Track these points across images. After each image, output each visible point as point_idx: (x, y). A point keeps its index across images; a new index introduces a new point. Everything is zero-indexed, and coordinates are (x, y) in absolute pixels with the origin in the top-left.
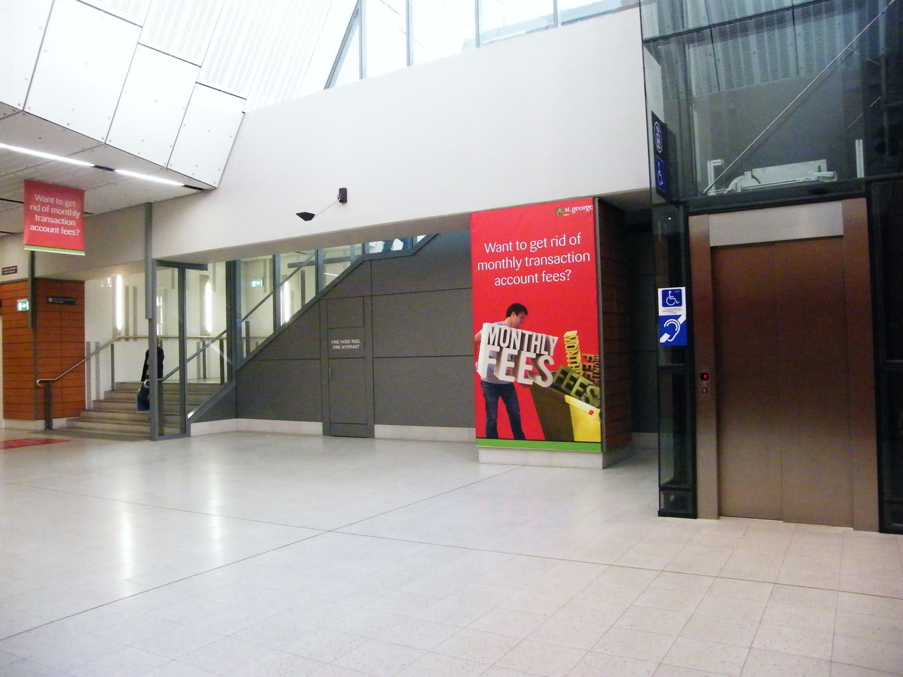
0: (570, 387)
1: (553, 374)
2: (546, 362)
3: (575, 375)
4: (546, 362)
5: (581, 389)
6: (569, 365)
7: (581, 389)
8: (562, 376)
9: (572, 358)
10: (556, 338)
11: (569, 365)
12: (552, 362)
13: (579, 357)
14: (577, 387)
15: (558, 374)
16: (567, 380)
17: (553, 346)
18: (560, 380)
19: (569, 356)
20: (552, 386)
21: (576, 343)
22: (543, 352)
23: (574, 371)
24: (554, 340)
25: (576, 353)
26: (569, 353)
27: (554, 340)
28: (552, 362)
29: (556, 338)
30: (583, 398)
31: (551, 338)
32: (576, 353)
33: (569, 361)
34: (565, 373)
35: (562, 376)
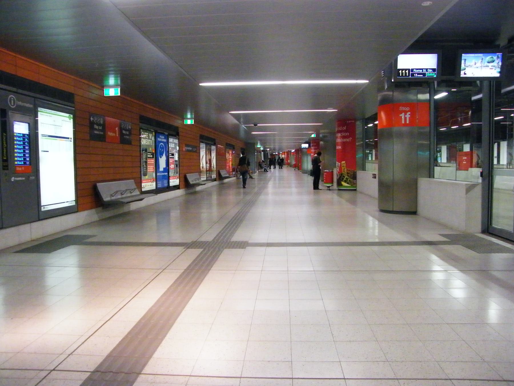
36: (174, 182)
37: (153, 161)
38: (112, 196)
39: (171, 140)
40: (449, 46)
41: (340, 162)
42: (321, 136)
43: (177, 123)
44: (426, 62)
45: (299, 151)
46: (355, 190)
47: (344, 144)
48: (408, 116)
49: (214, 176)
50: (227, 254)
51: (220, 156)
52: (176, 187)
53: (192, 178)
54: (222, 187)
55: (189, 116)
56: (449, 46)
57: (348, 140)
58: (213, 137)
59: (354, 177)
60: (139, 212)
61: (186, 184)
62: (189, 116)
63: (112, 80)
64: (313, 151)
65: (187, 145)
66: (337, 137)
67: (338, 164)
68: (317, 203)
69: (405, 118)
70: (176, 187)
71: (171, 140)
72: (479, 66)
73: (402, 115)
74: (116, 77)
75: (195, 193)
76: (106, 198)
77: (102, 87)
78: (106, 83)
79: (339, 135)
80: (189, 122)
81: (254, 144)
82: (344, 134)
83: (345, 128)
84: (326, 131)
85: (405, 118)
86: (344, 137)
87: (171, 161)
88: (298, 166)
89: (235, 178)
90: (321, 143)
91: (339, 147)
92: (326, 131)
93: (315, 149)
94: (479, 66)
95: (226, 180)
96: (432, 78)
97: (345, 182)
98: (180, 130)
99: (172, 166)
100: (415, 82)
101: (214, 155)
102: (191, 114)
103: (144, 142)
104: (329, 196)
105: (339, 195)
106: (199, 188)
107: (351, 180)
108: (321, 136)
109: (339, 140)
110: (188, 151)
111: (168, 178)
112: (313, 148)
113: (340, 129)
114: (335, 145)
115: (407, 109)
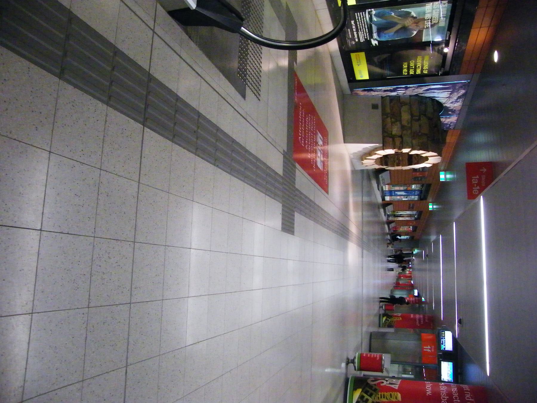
0: (366, 392)
1: (375, 385)
2: (383, 382)
3: (374, 396)
4: (383, 382)
5: (365, 399)
6: (380, 393)
7: (365, 399)
8: (373, 388)
9: (384, 395)
10: (397, 388)
11: (380, 393)
12: (382, 385)
13: (384, 400)
14: (366, 397)
15: (374, 387)
16: (371, 391)
17: (393, 386)
18: (371, 387)
19: (386, 393)
20: (368, 384)
21: (394, 400)
22: (388, 382)
23: (376, 396)
24: (396, 387)
25: (387, 399)
26: (387, 394)
27: (396, 387)
28: (382, 385)
29: (397, 388)
30: (360, 400)
31: (397, 386)
32: (387, 399)
33: (382, 393)
34: (375, 390)
35: (373, 388)
36: (387, 198)
37: (402, 188)
38: (382, 177)
39: (417, 197)
40: (456, 356)
41: (401, 316)
42: (423, 305)
43: (430, 199)
44: (448, 344)
45: (412, 287)
46: (380, 326)
47: (415, 319)
48: (428, 350)
49: (391, 219)
50: (360, 250)
51: (406, 223)
52: (383, 199)
53: (390, 208)
54: (381, 223)
55: (435, 207)
56: (456, 356)
57: (417, 322)
58: (421, 218)
59: (390, 326)
60: (370, 187)
61: (385, 205)
62: (435, 207)
63: (448, 176)
64: (411, 299)
65: (413, 205)
66: (419, 314)
67: (400, 314)
68: (369, 300)
69: (427, 349)
70: (383, 199)
71: (417, 197)
72: (447, 370)
73: (429, 347)
74: (450, 178)
75: (379, 208)
76: (380, 176)
77: (445, 171)
78: (447, 172)
79: (422, 316)
80: (431, 207)
81: (417, 247)
82: (422, 319)
83: (427, 321)
84: (427, 309)
85: (427, 349)
86: (420, 320)
87: (402, 197)
88: (397, 286)
89: (388, 231)
90: (417, 305)
91: (412, 316)
92: (427, 309)
93: (413, 301)
94: (447, 370)
95: (386, 226)
96: (440, 347)
97: (386, 319)
98: (424, 201)
99: (398, 197)
100: (438, 340)
101: (407, 219)
102: (436, 208)
103: (413, 187)
104: (376, 308)
105: (375, 315)
106: (382, 210)
107: (387, 324)
108: (423, 305)
109: (417, 316)
110: (410, 204)
111: (391, 195)
112: (414, 299)
113: (426, 318)
114: (414, 315)
115: (433, 350)
